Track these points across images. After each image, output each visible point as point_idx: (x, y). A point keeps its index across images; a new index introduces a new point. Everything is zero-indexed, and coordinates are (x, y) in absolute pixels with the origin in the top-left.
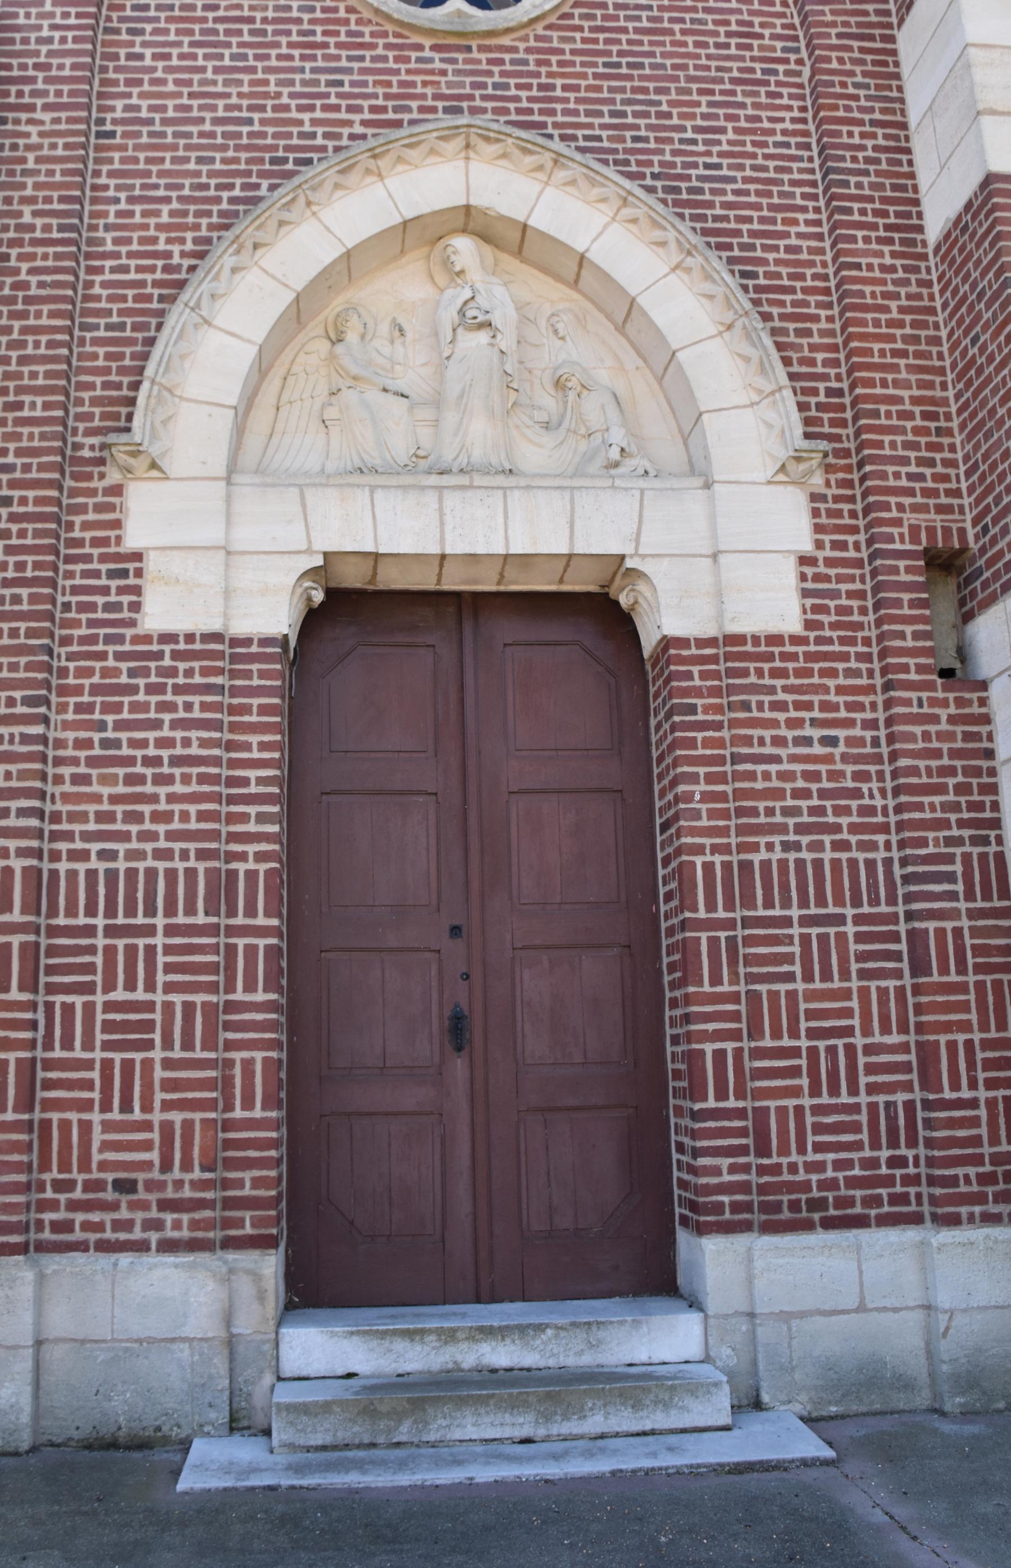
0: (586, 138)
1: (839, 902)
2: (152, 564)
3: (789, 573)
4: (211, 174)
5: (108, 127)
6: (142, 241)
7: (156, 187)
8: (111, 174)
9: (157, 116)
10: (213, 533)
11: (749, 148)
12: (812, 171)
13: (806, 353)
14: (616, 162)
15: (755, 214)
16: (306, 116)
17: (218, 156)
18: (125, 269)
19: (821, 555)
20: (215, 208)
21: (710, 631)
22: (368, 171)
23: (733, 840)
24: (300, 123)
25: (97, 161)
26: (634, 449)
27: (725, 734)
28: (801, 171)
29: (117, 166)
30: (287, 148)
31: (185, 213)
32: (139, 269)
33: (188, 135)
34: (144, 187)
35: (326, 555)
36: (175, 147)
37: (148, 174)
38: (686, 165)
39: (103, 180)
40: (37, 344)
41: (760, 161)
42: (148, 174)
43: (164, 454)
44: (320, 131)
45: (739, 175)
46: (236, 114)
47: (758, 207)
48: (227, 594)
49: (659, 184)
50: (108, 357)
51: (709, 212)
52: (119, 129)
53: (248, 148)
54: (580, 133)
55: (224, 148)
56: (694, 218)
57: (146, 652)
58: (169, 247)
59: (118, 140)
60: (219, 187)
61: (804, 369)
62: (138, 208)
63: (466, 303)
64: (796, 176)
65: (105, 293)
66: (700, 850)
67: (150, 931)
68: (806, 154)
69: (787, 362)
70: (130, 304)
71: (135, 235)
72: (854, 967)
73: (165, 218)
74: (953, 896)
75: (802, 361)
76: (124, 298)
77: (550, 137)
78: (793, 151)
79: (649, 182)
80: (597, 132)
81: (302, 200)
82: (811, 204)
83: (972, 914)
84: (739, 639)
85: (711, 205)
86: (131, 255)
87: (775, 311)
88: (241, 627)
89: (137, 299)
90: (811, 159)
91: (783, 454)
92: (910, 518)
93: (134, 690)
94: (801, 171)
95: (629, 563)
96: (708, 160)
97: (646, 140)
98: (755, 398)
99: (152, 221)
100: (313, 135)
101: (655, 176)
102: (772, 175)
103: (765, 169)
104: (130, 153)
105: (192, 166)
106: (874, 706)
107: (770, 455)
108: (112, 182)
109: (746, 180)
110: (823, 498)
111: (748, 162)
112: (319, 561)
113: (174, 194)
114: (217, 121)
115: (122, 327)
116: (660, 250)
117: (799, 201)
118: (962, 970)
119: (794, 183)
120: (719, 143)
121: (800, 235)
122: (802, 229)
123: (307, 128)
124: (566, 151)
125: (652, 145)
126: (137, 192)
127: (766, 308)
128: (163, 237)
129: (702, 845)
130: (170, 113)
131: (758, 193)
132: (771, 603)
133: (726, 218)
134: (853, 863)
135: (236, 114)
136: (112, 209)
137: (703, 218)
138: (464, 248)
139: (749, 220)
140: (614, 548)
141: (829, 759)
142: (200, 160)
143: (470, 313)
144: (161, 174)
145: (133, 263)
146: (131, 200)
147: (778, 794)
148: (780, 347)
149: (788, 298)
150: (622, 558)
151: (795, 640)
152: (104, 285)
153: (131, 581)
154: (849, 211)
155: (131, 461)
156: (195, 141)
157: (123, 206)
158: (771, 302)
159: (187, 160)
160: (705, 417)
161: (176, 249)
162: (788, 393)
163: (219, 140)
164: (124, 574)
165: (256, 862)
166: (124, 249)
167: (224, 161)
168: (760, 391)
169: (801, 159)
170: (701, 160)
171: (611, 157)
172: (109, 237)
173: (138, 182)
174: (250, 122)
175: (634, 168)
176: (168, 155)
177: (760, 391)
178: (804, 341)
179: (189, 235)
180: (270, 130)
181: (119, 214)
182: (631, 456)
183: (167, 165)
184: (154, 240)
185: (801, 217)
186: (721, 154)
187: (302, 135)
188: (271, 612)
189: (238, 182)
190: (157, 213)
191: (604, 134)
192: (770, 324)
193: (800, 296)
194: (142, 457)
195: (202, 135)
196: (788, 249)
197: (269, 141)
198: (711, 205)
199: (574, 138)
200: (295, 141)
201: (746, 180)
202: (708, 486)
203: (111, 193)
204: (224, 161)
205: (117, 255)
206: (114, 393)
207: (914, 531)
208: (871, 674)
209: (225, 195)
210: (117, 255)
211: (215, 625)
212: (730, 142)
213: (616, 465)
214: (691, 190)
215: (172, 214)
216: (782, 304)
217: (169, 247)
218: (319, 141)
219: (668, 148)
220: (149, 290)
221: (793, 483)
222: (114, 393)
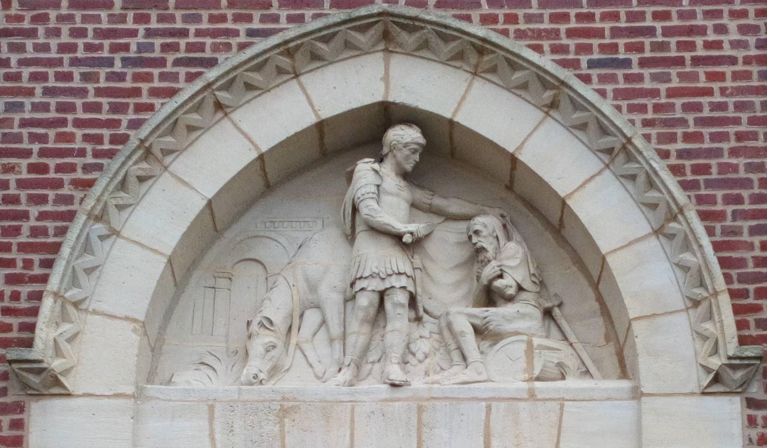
22: (280, 71)
43: (66, 372)
194: (44, 375)
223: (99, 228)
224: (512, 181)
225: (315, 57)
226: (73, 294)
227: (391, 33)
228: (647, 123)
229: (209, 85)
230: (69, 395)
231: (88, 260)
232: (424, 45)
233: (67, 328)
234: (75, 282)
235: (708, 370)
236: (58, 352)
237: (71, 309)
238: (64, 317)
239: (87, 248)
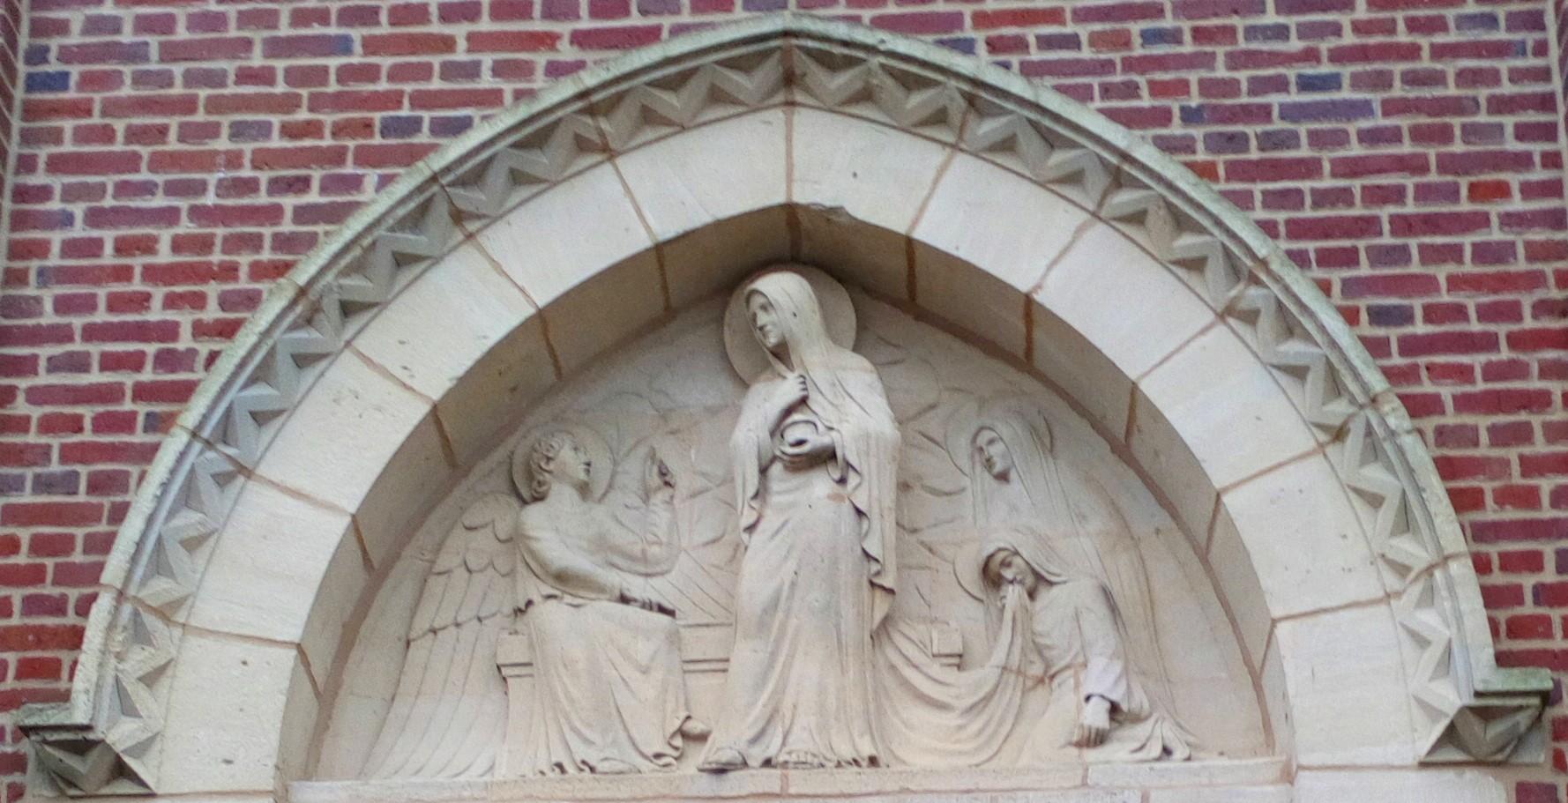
0: (1046, 43)
4: (261, 160)
5: (53, 67)
6: (115, 303)
7: (147, 189)
8: (57, 164)
9: (154, 41)
11: (1403, 37)
12: (1544, 75)
13: (1517, 479)
14: (1107, 91)
15: (1409, 182)
16: (460, 31)
17: (276, 120)
18: (78, 363)
20: (267, 231)
24: (447, 44)
25: (28, 137)
26: (1137, 701)
28: (1517, 76)
29: (68, 147)
30: (420, 100)
31: (205, 244)
32: (111, 363)
33: (216, 79)
34: (123, 189)
36: (188, 105)
37: (132, 162)
38: (1259, 86)
39: (39, 178)
41: (1425, 63)
42: (132, 162)
43: (141, 749)
44: (487, 60)
45: (1376, 98)
46: (316, 30)
47: (1415, 165)
49: (1198, 132)
50: (39, 545)
51: (1305, 185)
52: (75, 71)
53: (339, 102)
54: (1031, 33)
55: (288, 103)
56: (1272, 200)
58: (171, 315)
59: (72, 94)
60: (278, 186)
61: (1511, 514)
62: (109, 236)
64: (1507, 89)
65: (36, 412)
68: (1530, 38)
69: (1463, 501)
70: (87, 436)
71: (102, 293)
73: (164, 256)
75: (1507, 496)
76: (76, 425)
77: (966, 47)
78: (1501, 35)
79: (1176, 129)
80: (1069, 29)
81: (441, 210)
82: (1537, 148)
85: (1309, 168)
86: (91, 333)
87: (1447, 391)
89: (101, 424)
90: (1541, 49)
91: (1451, 698)
94: (1517, 76)
96: (1309, 70)
97: (1174, 37)
98: (1392, 581)
99: (138, 262)
100: (472, 71)
101: (1190, 116)
102: (1452, 90)
103: (1437, 79)
104: (96, 120)
105: (223, 144)
107: (1422, 704)
108: (57, 182)
109: (1391, 108)
111: (1398, 68)
113: (183, 204)
114: (277, 47)
115: (67, 483)
116: (1193, 279)
117: (1512, 145)
119: (1501, 105)
120: (1337, 30)
121: (1509, 220)
122: (1517, 204)
123: (461, 55)
124: (994, 77)
125: (1188, 47)
126: (108, 202)
127: (1427, 387)
128: (159, 293)
130: (182, 34)
131: (1419, 134)
133: (1344, 196)
135: (316, 30)
136: (56, 238)
137: (1290, 199)
138: (783, 291)
139: (1397, 195)
142: (238, 131)
143: (793, 434)
144: (158, 163)
145: (95, 349)
146: (96, 218)
148: (1447, 468)
149: (1478, 360)
152: (35, 396)
155: (72, 762)
156: (231, 89)
157: (79, 231)
158: (1436, 372)
159: (212, 131)
160: (1283, 630)
161: (185, 319)
162: (1462, 569)
163: (280, 88)
166: (77, 322)
167: (289, 131)
168: (1402, 570)
169: (1520, 49)
170: (1291, 73)
171: (1095, 82)
172: (48, 296)
173: (110, 180)
174: (343, 45)
175: (1146, 101)
176: (174, 122)
177: (1402, 570)
178: (1512, 454)
179: (212, 290)
180: (386, 62)
181: (71, 248)
182: (1136, 718)
183: (173, 144)
184: (142, 301)
185: (1514, 179)
186: (1338, 56)
187: (450, 71)
189: (316, 175)
190: (148, 246)
191: (1084, 31)
192: (1430, 423)
193: (1505, 354)
194: (94, 754)
195: (245, 76)
196: (1483, 253)
197: (383, 85)
198: (1309, 168)
199: (1019, 45)
200: (436, 84)
201: (1391, 108)
202: (1288, 775)
203: (55, 205)
204: (289, 131)
205: (63, 334)
206: (50, 621)
209: (289, 202)
210: (63, 334)
212: (1358, 28)
213: (1097, 739)
214: (1268, 141)
215: (178, 245)
216: (1464, 373)
217: (171, 315)
218: (486, 81)
219: (1221, 51)
220: (127, 406)
221: (1478, 763)
222: (50, 621)
223: (214, 460)
224: (1029, 351)
226: (159, 589)
227: (788, 71)
228: (1298, 230)
229: (434, 178)
230: (152, 795)
233: (139, 660)
234: (160, 566)
235: (1432, 712)
236: (127, 708)
237: (151, 621)
238: (140, 635)
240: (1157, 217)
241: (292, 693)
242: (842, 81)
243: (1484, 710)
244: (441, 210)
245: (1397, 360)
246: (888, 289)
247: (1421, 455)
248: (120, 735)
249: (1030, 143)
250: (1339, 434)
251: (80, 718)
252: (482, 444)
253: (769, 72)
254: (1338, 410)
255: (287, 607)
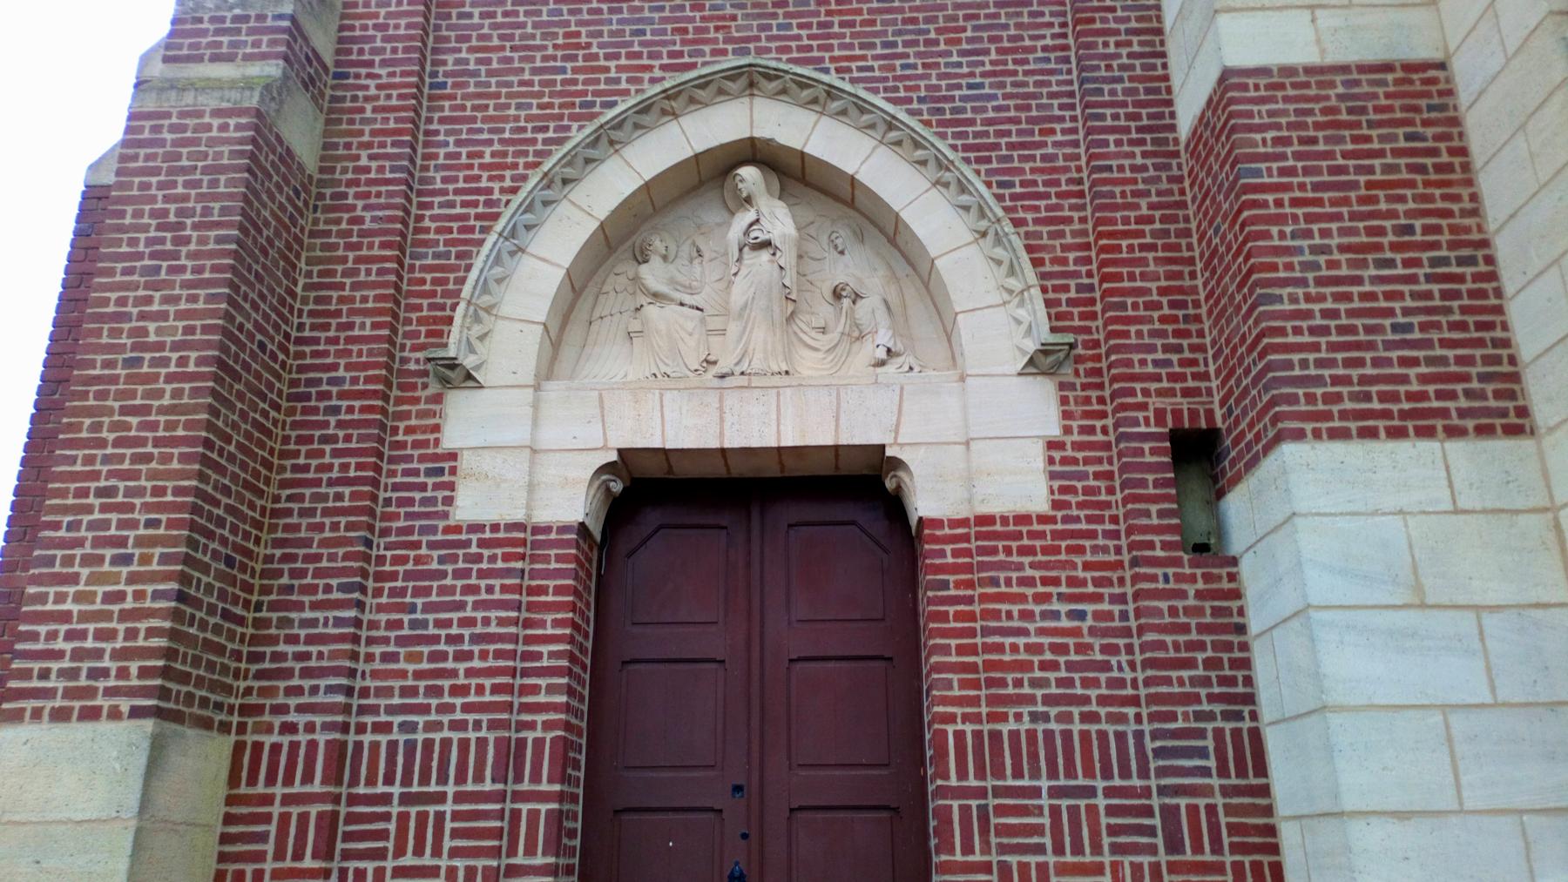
0: (860, 69)
1: (1089, 773)
2: (466, 462)
3: (1036, 457)
4: (529, 119)
5: (441, 79)
6: (467, 179)
7: (480, 131)
8: (442, 121)
9: (483, 68)
10: (519, 434)
11: (1011, 67)
12: (1070, 83)
13: (1059, 254)
14: (886, 90)
15: (1013, 128)
16: (612, 64)
17: (535, 102)
18: (451, 205)
19: (1068, 439)
20: (531, 149)
21: (962, 512)
23: (984, 710)
24: (607, 70)
25: (430, 109)
26: (899, 347)
27: (976, 608)
28: (1059, 83)
29: (447, 113)
30: (596, 93)
31: (504, 154)
32: (465, 204)
33: (509, 84)
34: (470, 131)
35: (621, 451)
36: (497, 95)
37: (473, 120)
38: (950, 87)
39: (434, 127)
40: (368, 272)
41: (1020, 78)
42: (473, 120)
43: (478, 367)
44: (624, 76)
45: (999, 92)
46: (552, 64)
47: (1016, 121)
48: (531, 487)
49: (924, 107)
50: (435, 281)
51: (970, 129)
52: (450, 81)
53: (561, 94)
54: (854, 65)
55: (540, 95)
56: (956, 136)
57: (455, 540)
58: (490, 184)
59: (448, 91)
60: (535, 130)
61: (1057, 268)
62: (464, 151)
63: (751, 225)
64: (1055, 88)
65: (433, 225)
66: (951, 719)
67: (440, 798)
68: (1065, 67)
69: (1036, 263)
70: (455, 235)
71: (461, 175)
72: (1106, 841)
73: (487, 159)
74: (1205, 772)
75: (1054, 261)
76: (450, 231)
77: (826, 71)
78: (1052, 66)
79: (915, 106)
80: (870, 63)
81: (604, 140)
82: (1067, 114)
83: (1226, 791)
84: (987, 520)
85: (972, 122)
86: (457, 192)
87: (1029, 216)
88: (542, 516)
89: (461, 230)
90: (1069, 72)
91: (1031, 346)
92: (1155, 402)
93: (444, 575)
94: (1059, 83)
95: (889, 452)
96: (971, 81)
97: (914, 67)
98: (1006, 296)
99: (476, 162)
100: (617, 81)
101: (921, 100)
102: (1032, 89)
103: (1025, 84)
104: (459, 102)
105: (512, 112)
106: (1121, 581)
107: (1019, 349)
108: (442, 128)
109: (1006, 96)
110: (1072, 387)
111: (1009, 80)
112: (613, 457)
113: (495, 137)
114: (535, 71)
115: (447, 255)
116: (922, 169)
117: (1057, 112)
118: (1217, 848)
119: (1052, 95)
120: (983, 64)
121: (1056, 144)
122: (1059, 137)
123: (613, 74)
124: (838, 83)
125: (920, 71)
126: (464, 136)
127: (1021, 215)
128: (485, 175)
129: (953, 717)
130: (495, 65)
131: (1017, 108)
132: (1020, 486)
133: (986, 134)
134: (1102, 735)
135: (552, 64)
136: (442, 151)
137: (963, 135)
138: (749, 175)
139: (1009, 133)
140: (875, 439)
141: (1076, 632)
142: (519, 107)
143: (753, 235)
144: (485, 120)
145: (458, 199)
146: (459, 143)
147: (1025, 666)
148: (1030, 249)
149: (1042, 203)
150: (883, 446)
151: (1043, 519)
152: (433, 218)
153: (446, 478)
154: (1102, 117)
155: (448, 372)
156: (516, 89)
157: (451, 149)
158: (1025, 208)
159: (508, 106)
160: (960, 317)
161: (496, 186)
162: (1036, 292)
163: (537, 88)
164: (441, 471)
165: (541, 732)
166: (451, 187)
167: (540, 106)
168: (1010, 292)
169: (1060, 72)
170: (963, 82)
171: (881, 86)
172: (438, 176)
173: (465, 127)
174: (563, 70)
175: (902, 94)
176: (491, 103)
177: (1010, 292)
178: (1057, 243)
179: (508, 173)
180: (581, 77)
181: (448, 156)
182: (898, 355)
183: (491, 112)
184: (478, 178)
185: (1058, 127)
186: (983, 75)
187: (609, 81)
188: (569, 501)
189: (552, 125)
190: (480, 155)
191: (876, 64)
192: (1022, 230)
193: (1054, 200)
195: (522, 83)
196: (1044, 158)
197: (580, 87)
198: (972, 122)
199: (849, 70)
200: (602, 87)
201: (1006, 96)
202: (962, 379)
203: (441, 138)
204: (540, 106)
205: (444, 192)
206: (439, 313)
207: (1160, 415)
208: (1118, 550)
209: (540, 136)
210: (444, 192)
211: (519, 516)
212: (991, 63)
213: (882, 363)
214: (954, 110)
215: (493, 155)
216: (1036, 209)
217: (490, 184)
218: (624, 85)
219: (934, 73)
220: (472, 222)
221: (1043, 374)
222: (439, 313)
225: (692, 101)
226: (485, 300)
227: (750, 81)
228: (966, 148)
231: (497, 271)
232: (784, 91)
233: (477, 330)
234: (486, 290)
235: (1023, 352)
236: (472, 350)
237: (482, 314)
238: (477, 319)
239: (498, 261)
240: (907, 143)
241: (541, 344)
242: (773, 86)
243: (1045, 351)
244: (604, 140)
245: (1008, 203)
246: (793, 173)
247: (1018, 243)
248: (469, 362)
249: (853, 111)
250: (984, 234)
251: (452, 354)
252: (622, 239)
253: (743, 81)
254: (983, 224)
255: (540, 309)
